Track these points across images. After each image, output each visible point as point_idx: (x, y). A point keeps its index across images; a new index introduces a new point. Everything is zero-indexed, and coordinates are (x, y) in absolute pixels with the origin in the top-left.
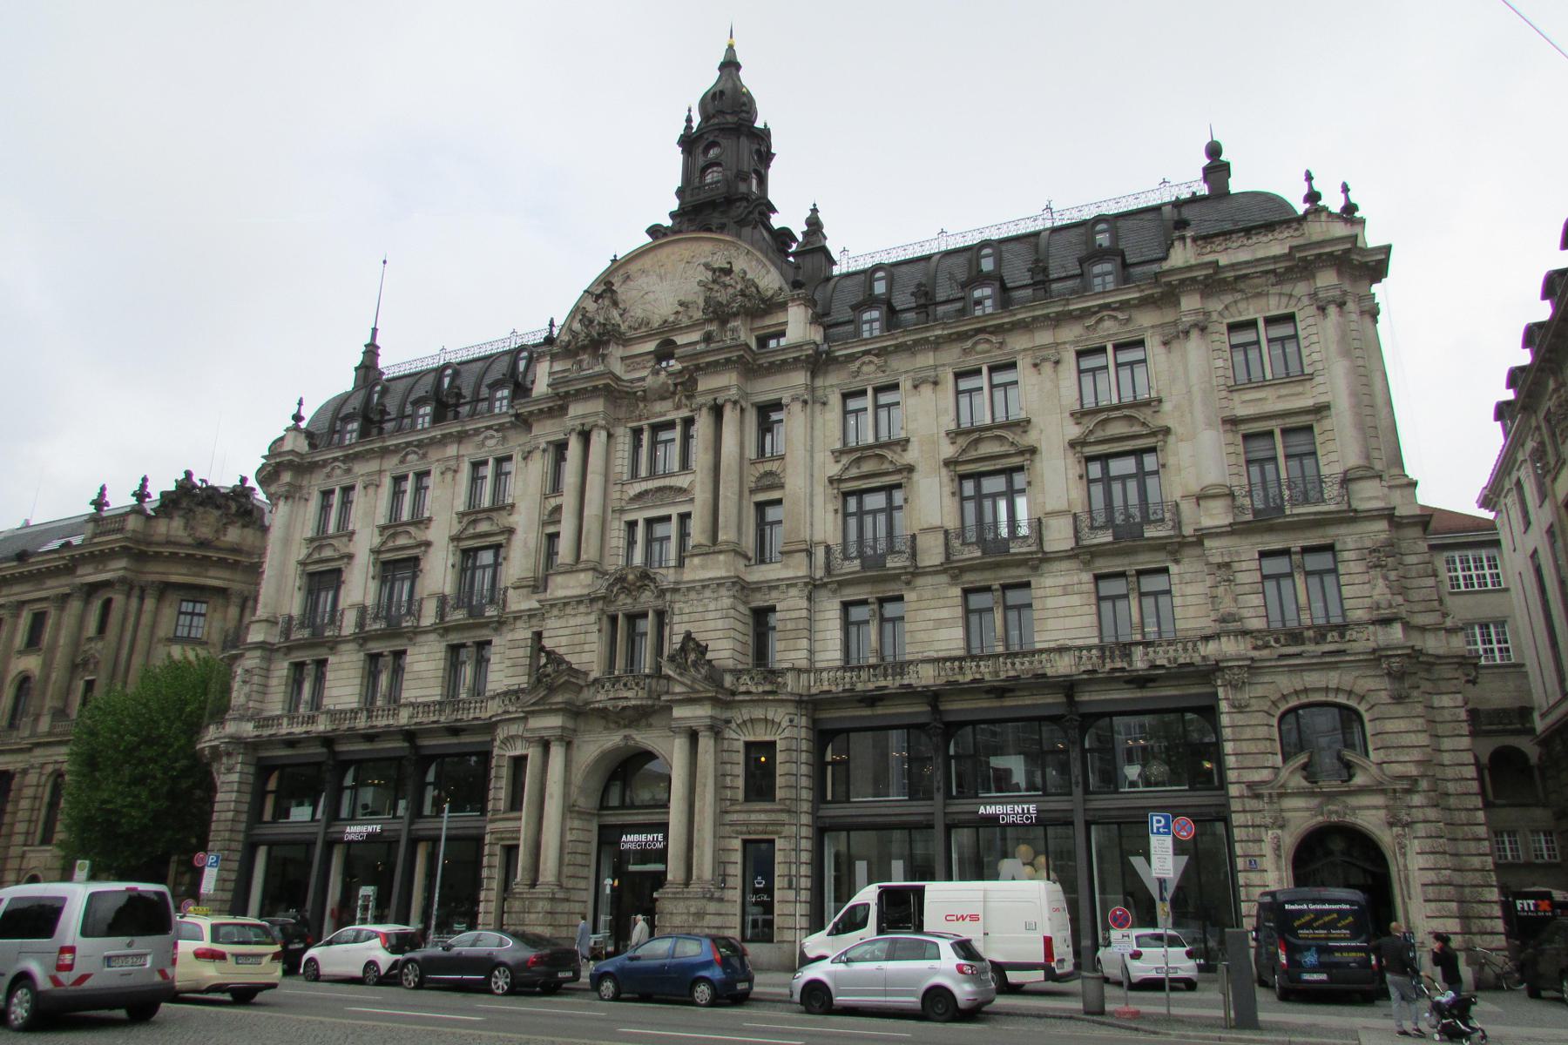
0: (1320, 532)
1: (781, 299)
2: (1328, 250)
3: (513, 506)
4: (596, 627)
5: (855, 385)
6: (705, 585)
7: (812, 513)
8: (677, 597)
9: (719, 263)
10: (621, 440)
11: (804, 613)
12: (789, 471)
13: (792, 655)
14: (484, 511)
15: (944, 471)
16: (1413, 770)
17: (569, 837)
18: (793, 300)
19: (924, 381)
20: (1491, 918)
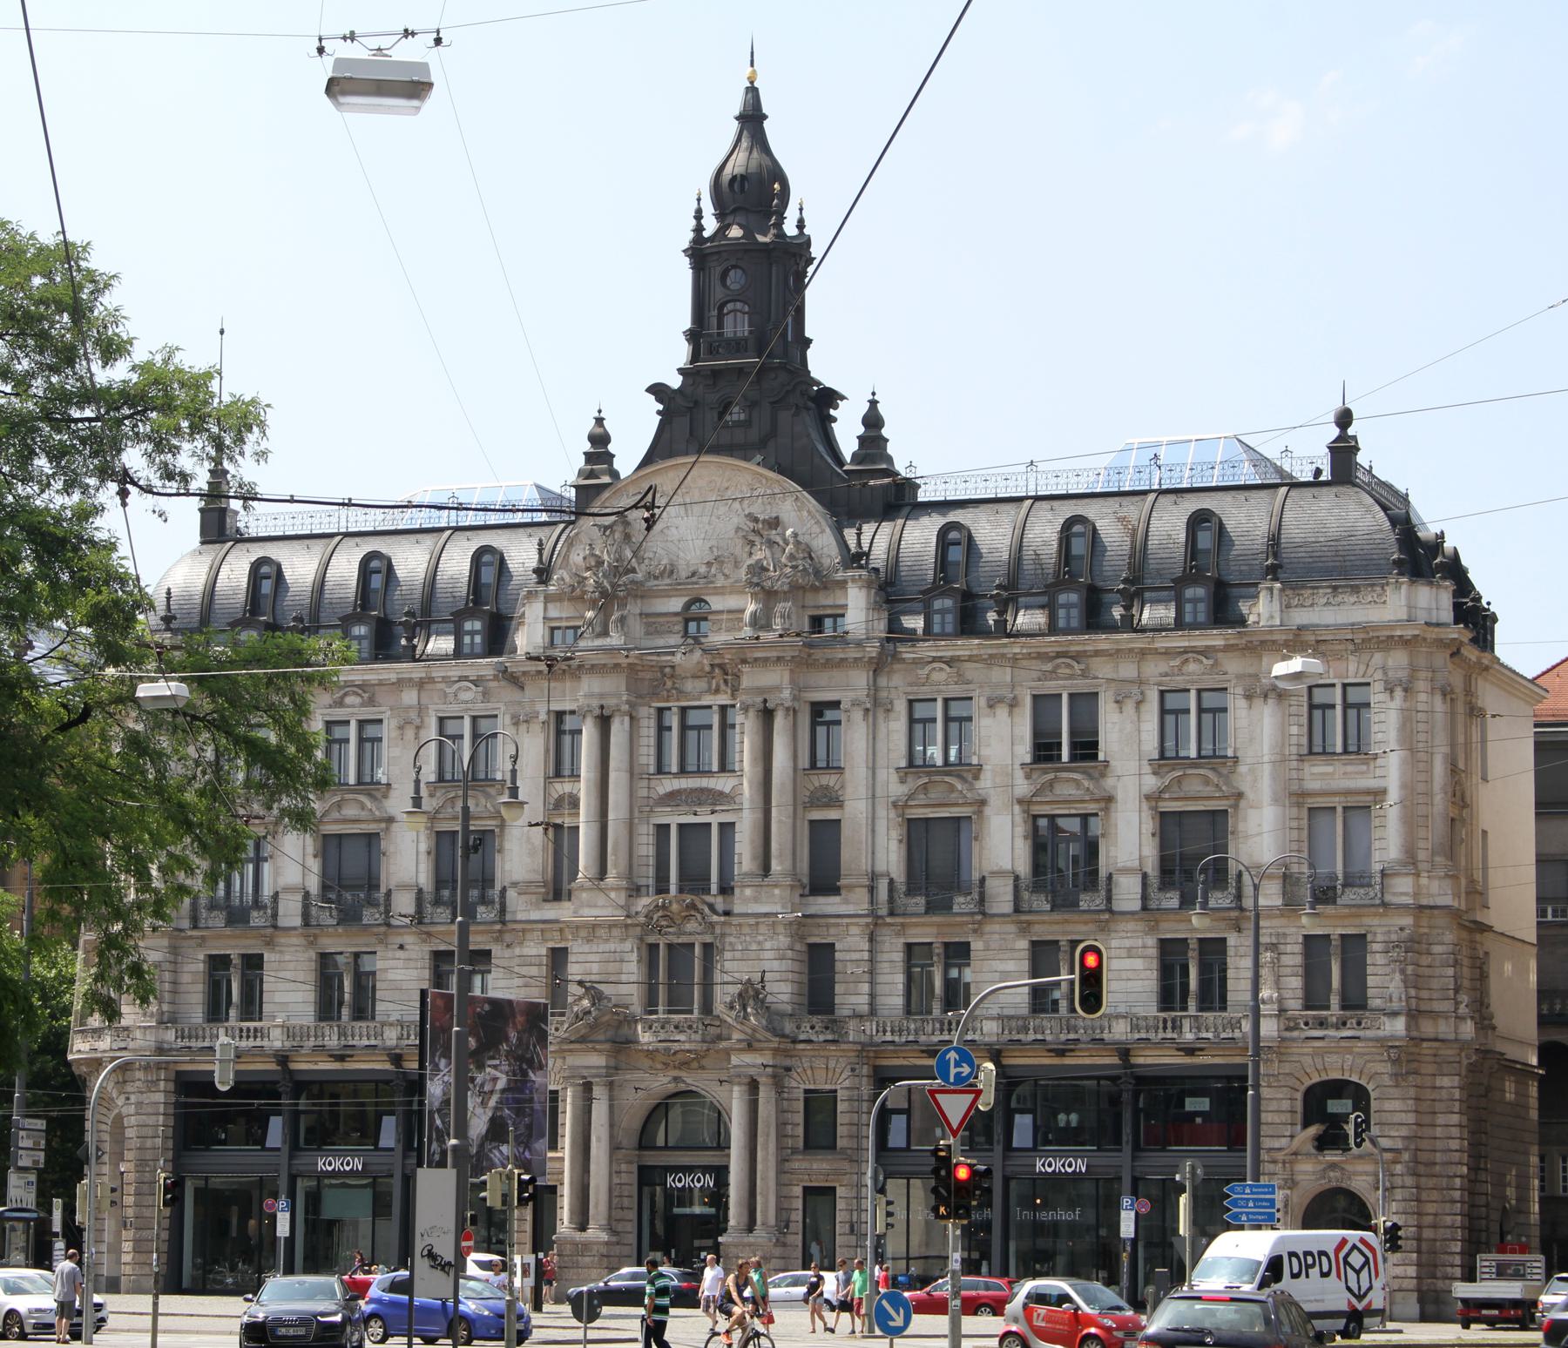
0: (1357, 921)
1: (840, 575)
2: (1398, 633)
5: (924, 692)
7: (873, 846)
9: (762, 511)
10: (644, 723)
11: (866, 956)
13: (853, 999)
15: (1017, 808)
16: (1399, 1144)
17: (616, 1180)
18: (854, 580)
19: (1000, 700)
20: (1452, 1266)
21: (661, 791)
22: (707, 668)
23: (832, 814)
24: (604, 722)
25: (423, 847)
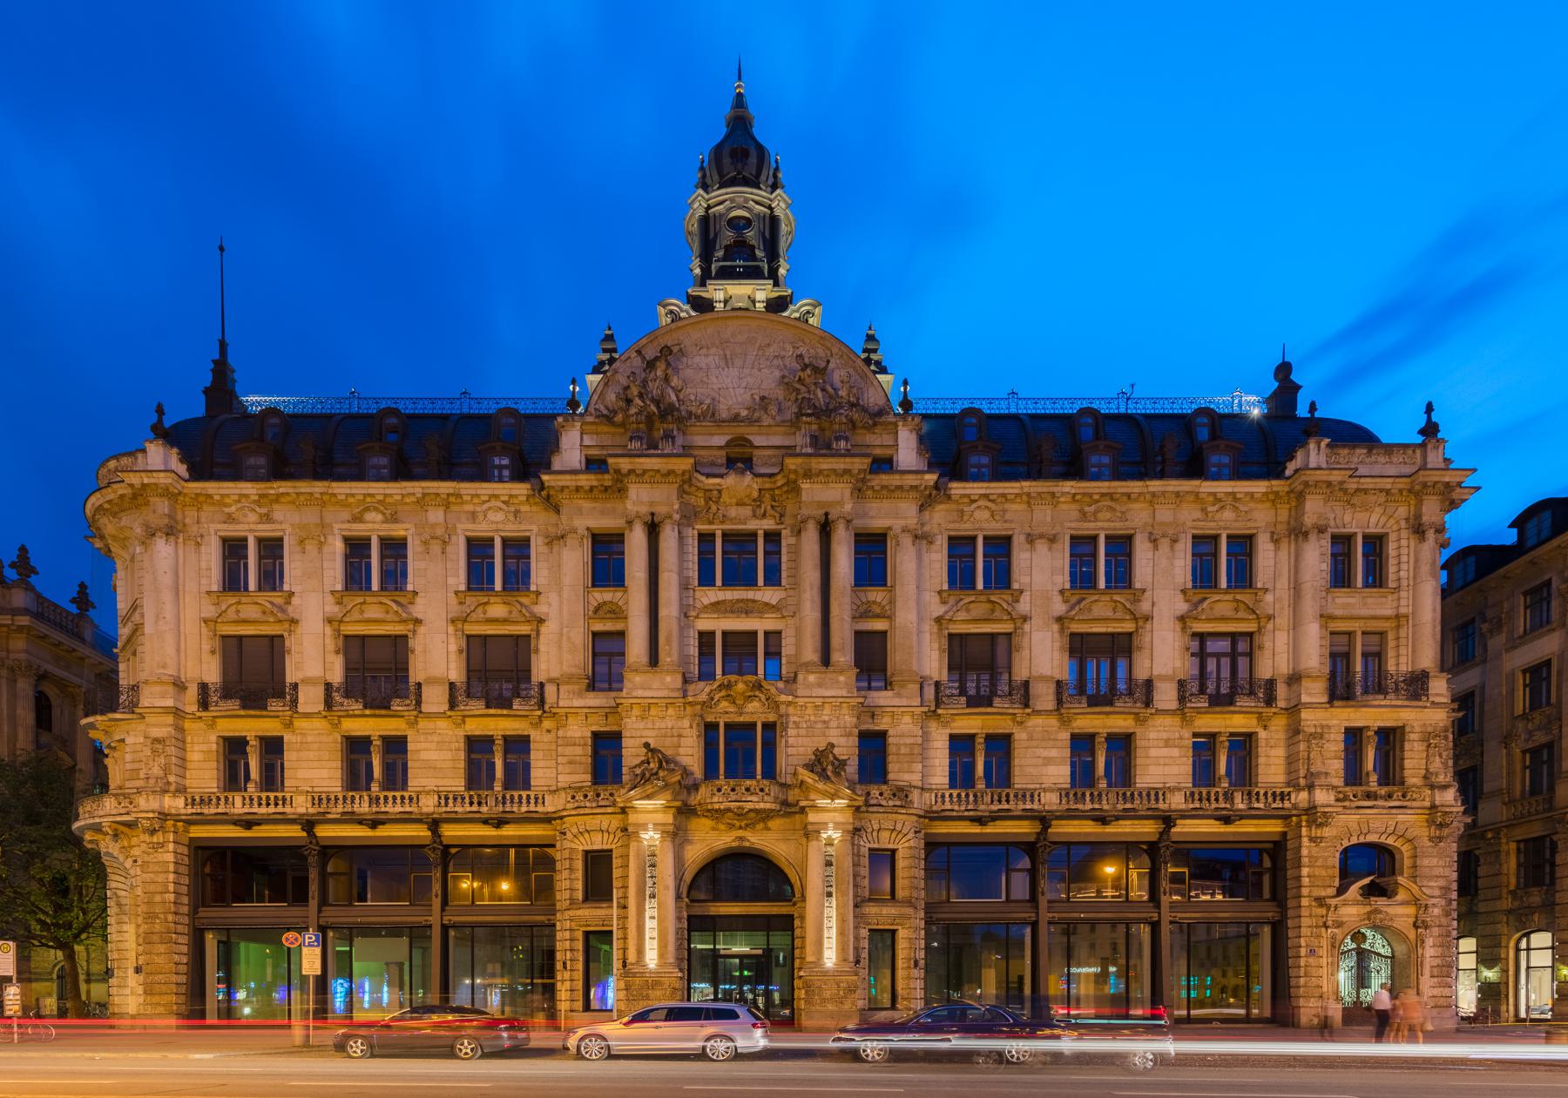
8: (791, 710)
11: (919, 740)
12: (899, 604)
21: (706, 601)
22: (755, 494)
23: (879, 625)
24: (653, 529)
25: (453, 647)
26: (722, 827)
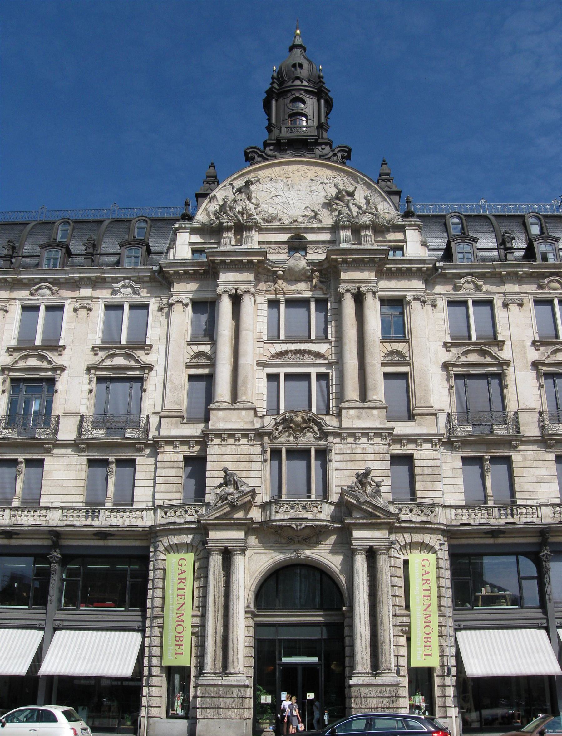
1: (400, 222)
3: (151, 347)
4: (261, 458)
6: (365, 433)
13: (431, 494)
14: (122, 347)
18: (410, 225)
21: (273, 352)
22: (309, 274)
26: (283, 541)
